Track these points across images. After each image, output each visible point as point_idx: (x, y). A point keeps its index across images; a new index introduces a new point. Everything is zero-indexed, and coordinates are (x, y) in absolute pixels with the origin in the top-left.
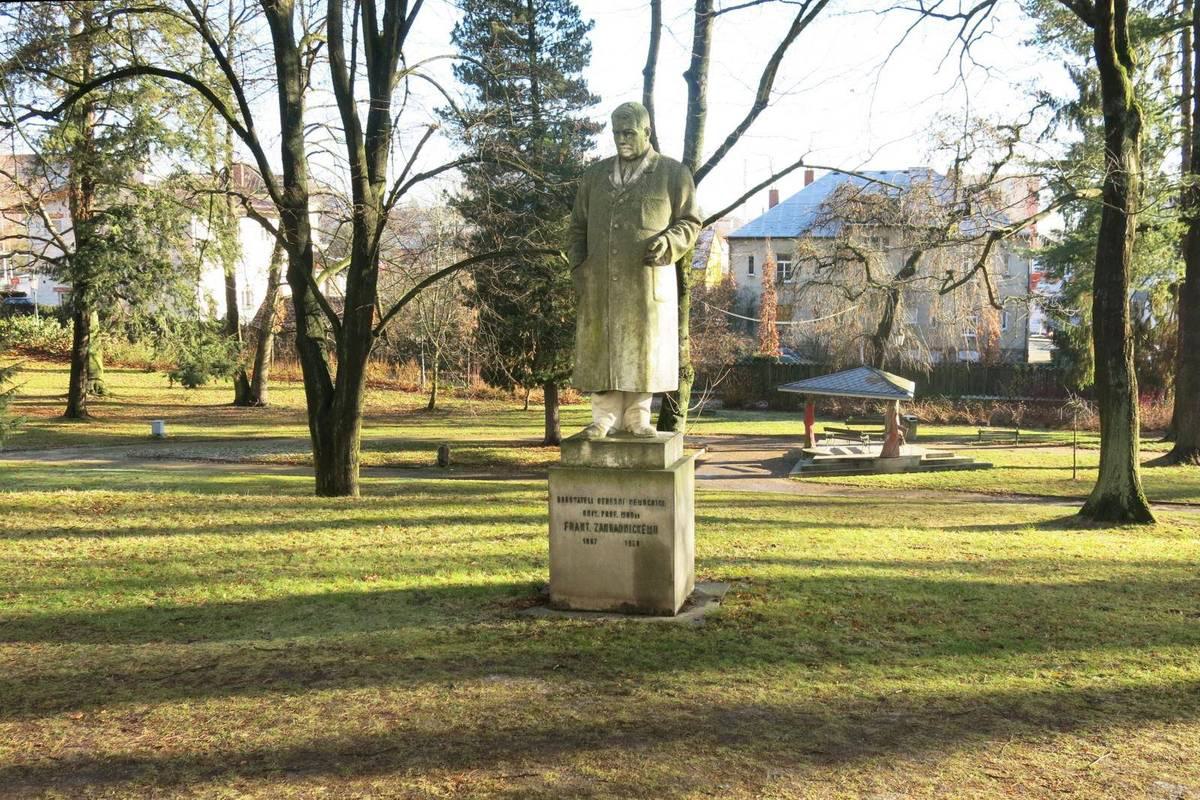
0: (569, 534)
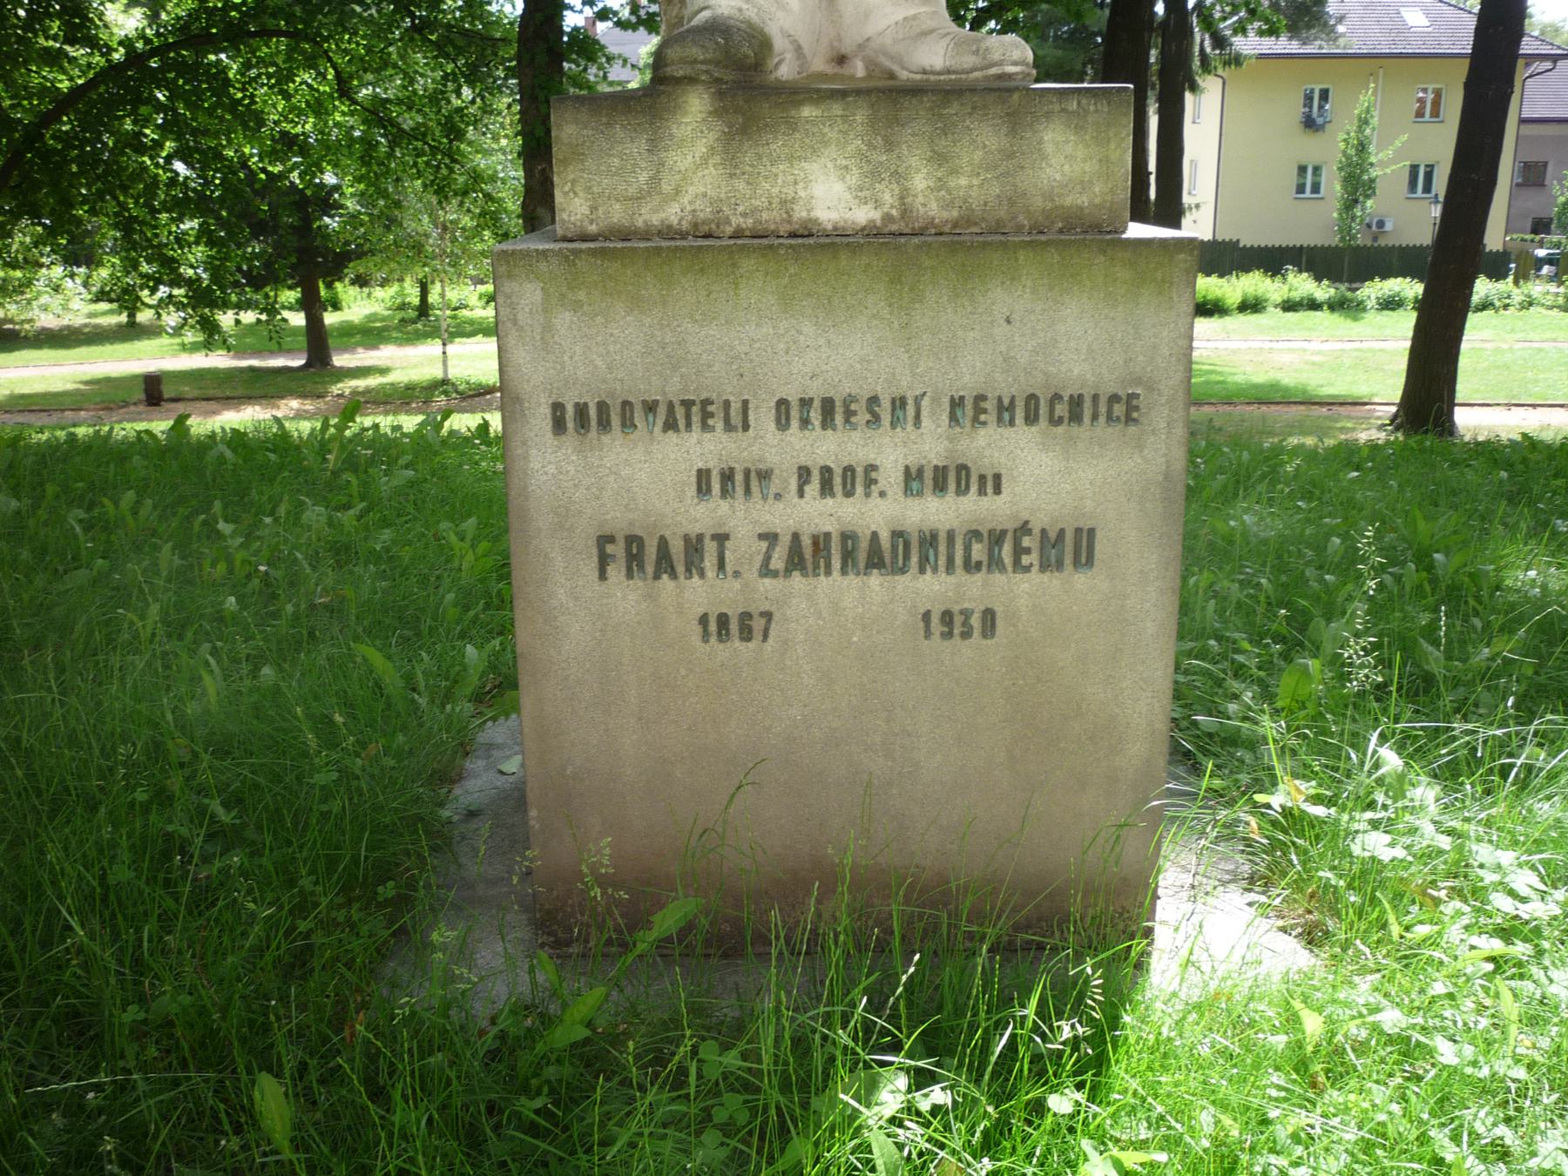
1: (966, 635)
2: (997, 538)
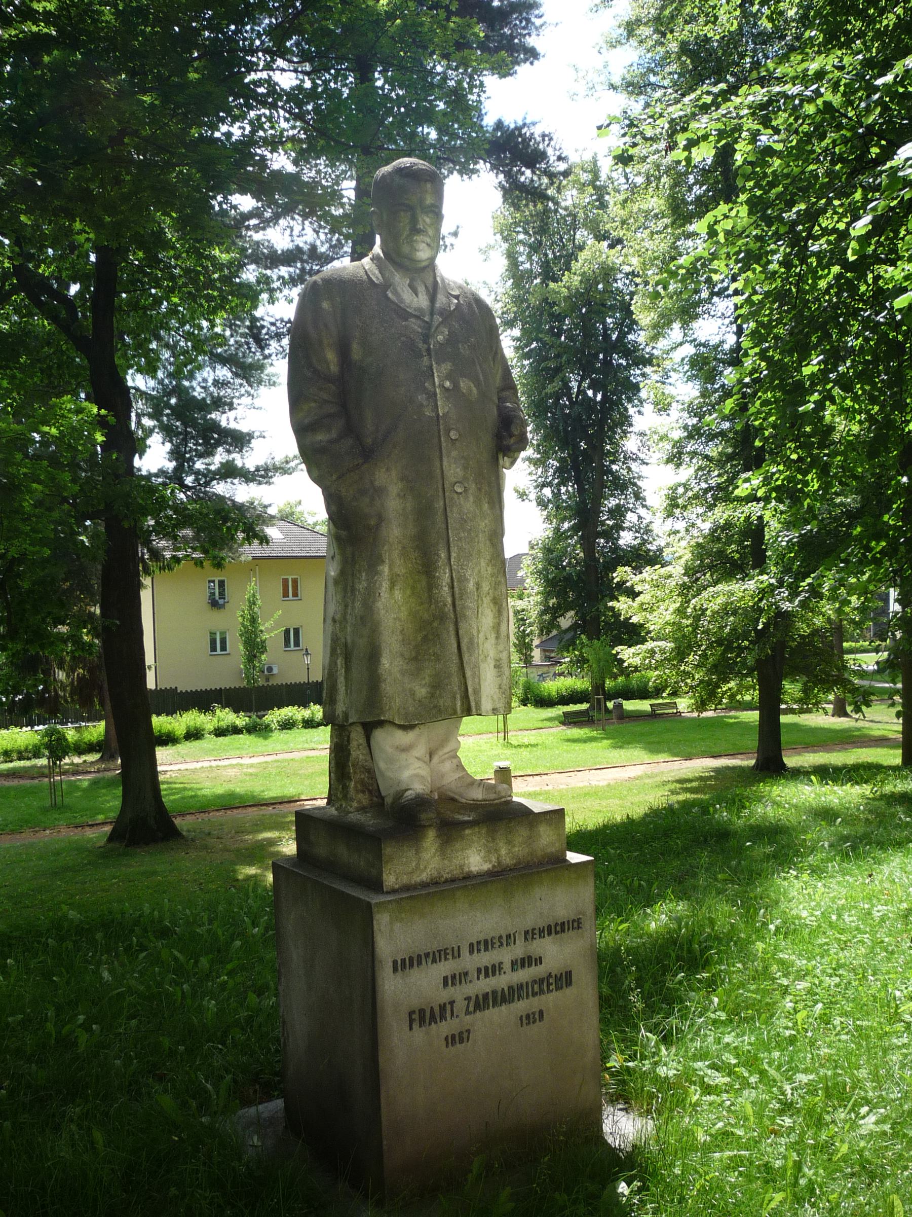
0: (419, 1035)
1: (534, 1022)
2: (541, 981)
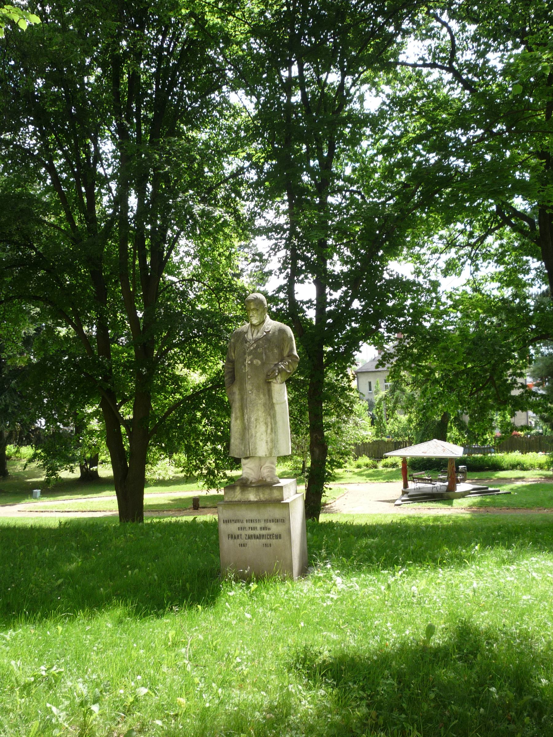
0: (231, 541)
